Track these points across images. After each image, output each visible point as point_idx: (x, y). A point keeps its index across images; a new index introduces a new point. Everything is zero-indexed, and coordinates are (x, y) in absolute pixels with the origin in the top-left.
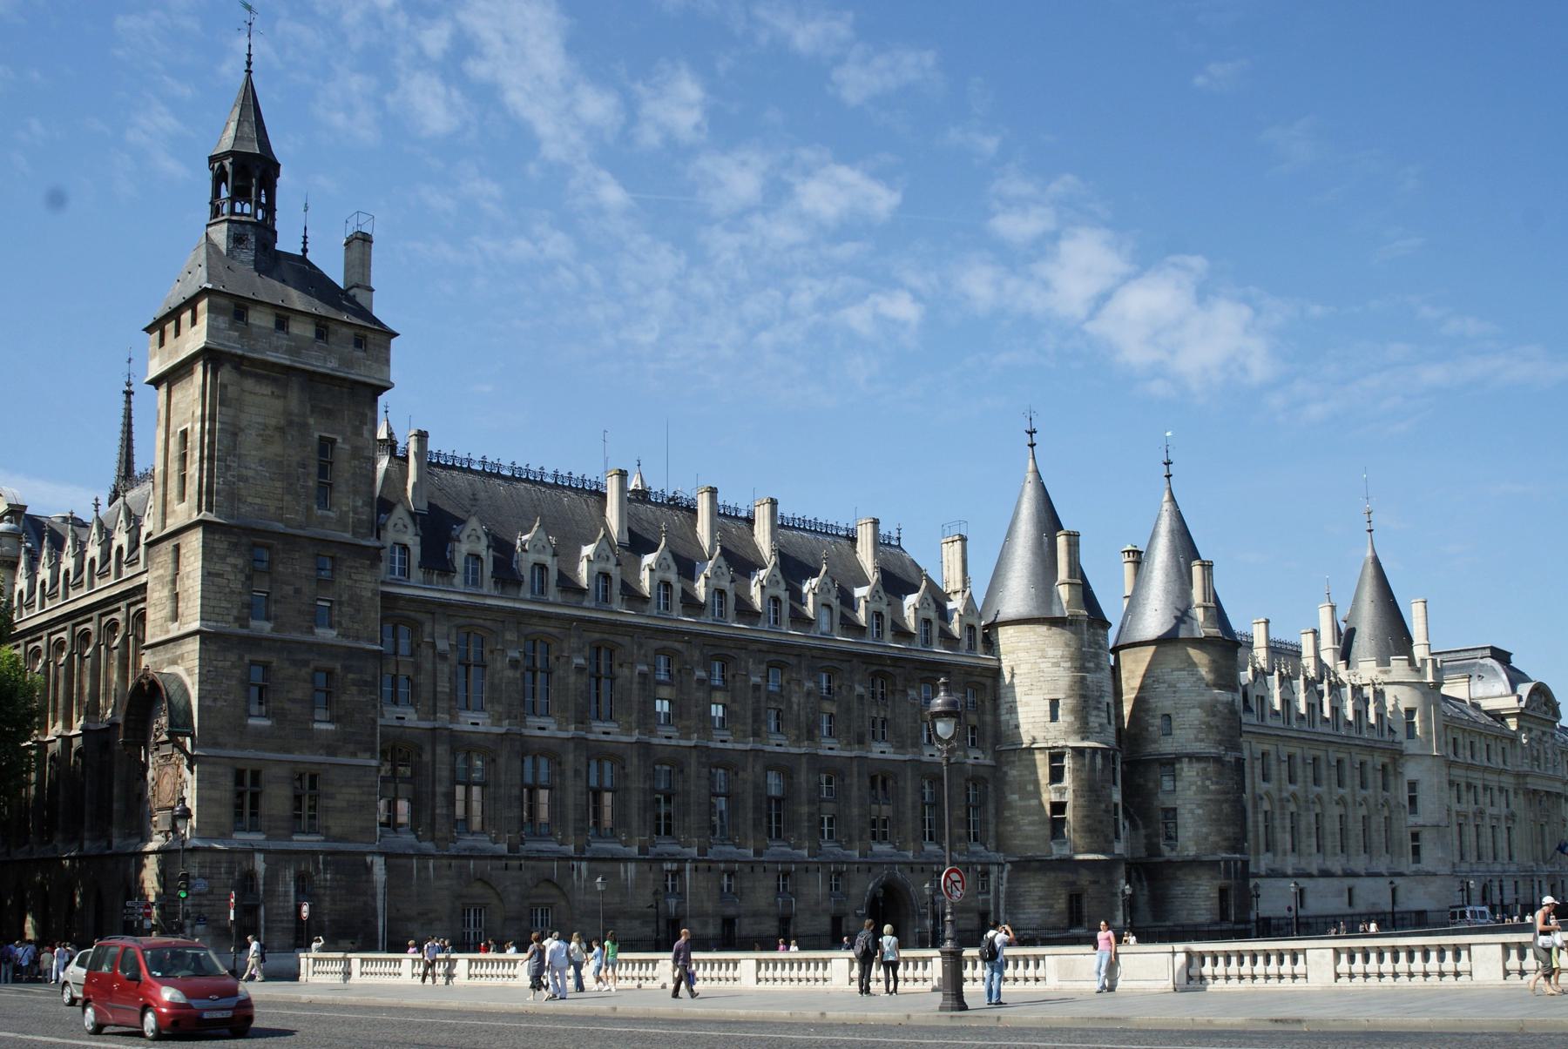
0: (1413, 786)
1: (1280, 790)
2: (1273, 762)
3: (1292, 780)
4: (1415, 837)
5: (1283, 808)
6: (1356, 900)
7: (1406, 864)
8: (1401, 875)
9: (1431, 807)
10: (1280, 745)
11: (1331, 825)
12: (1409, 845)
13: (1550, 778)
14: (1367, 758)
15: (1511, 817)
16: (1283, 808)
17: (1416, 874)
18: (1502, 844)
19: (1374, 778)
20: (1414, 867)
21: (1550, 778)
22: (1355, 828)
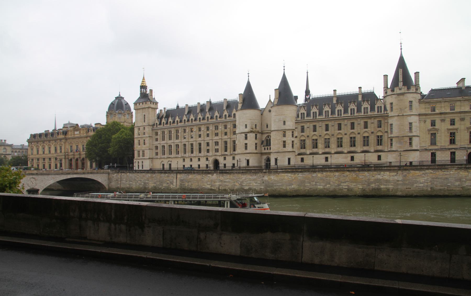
0: (391, 125)
9: (396, 132)
10: (320, 123)
11: (346, 141)
14: (369, 121)
20: (389, 150)
22: (359, 140)
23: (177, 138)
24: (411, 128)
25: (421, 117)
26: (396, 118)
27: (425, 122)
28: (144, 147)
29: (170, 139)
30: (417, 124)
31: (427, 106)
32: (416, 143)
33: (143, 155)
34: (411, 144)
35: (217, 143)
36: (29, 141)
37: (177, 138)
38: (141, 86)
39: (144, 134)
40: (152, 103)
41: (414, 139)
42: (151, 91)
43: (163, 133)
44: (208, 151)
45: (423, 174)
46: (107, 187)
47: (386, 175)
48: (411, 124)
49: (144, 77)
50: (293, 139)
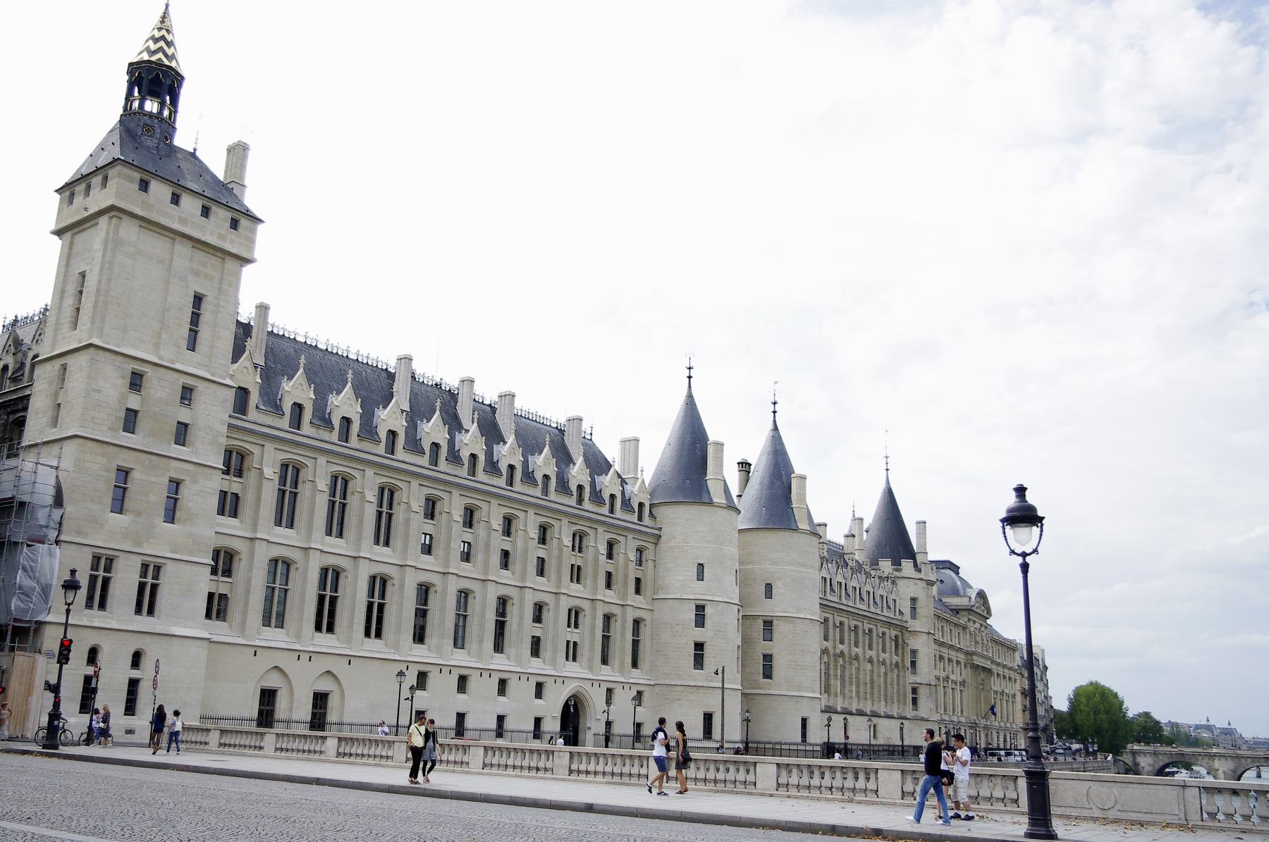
0: (914, 652)
1: (835, 648)
2: (831, 627)
3: (842, 642)
4: (914, 691)
5: (836, 661)
6: (879, 735)
7: (909, 713)
8: (906, 718)
9: (926, 671)
12: (910, 696)
13: (986, 658)
15: (963, 683)
16: (836, 661)
17: (915, 719)
18: (958, 702)
19: (890, 645)
20: (913, 714)
21: (986, 658)
23: (383, 535)
26: (924, 637)
28: (163, 541)
29: (336, 523)
33: (146, 600)
35: (574, 617)
37: (383, 535)
38: (133, 68)
39: (182, 433)
42: (238, 153)
43: (290, 474)
44: (536, 647)
49: (164, 17)
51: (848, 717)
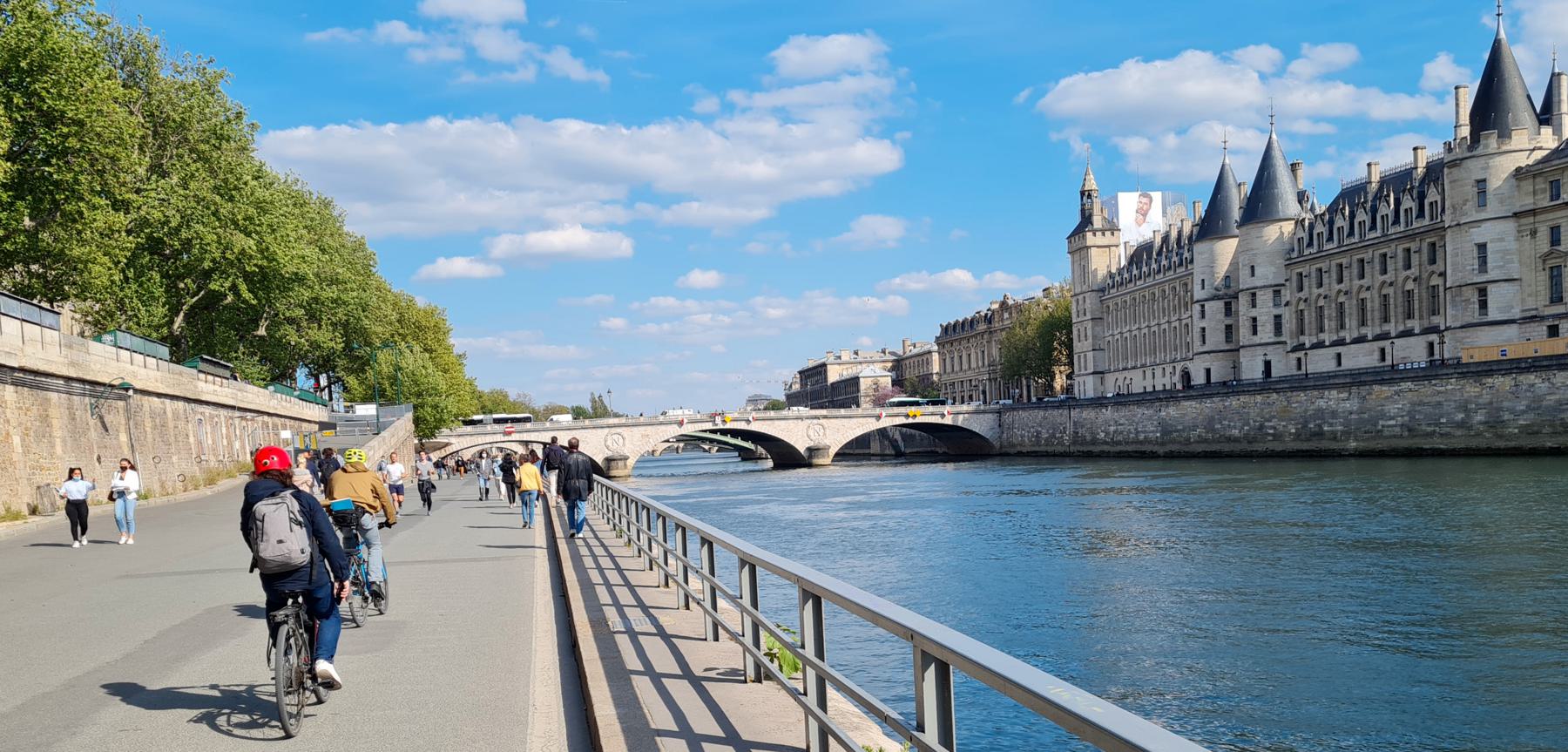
14: (1413, 246)
24: (1483, 261)
25: (1524, 221)
27: (1534, 233)
30: (1512, 245)
31: (1542, 184)
32: (1501, 301)
34: (1483, 305)
36: (938, 340)
40: (1099, 234)
41: (1491, 289)
45: (1396, 393)
46: (997, 444)
47: (1332, 399)
48: (1482, 247)
50: (1277, 311)
51: (1339, 349)
